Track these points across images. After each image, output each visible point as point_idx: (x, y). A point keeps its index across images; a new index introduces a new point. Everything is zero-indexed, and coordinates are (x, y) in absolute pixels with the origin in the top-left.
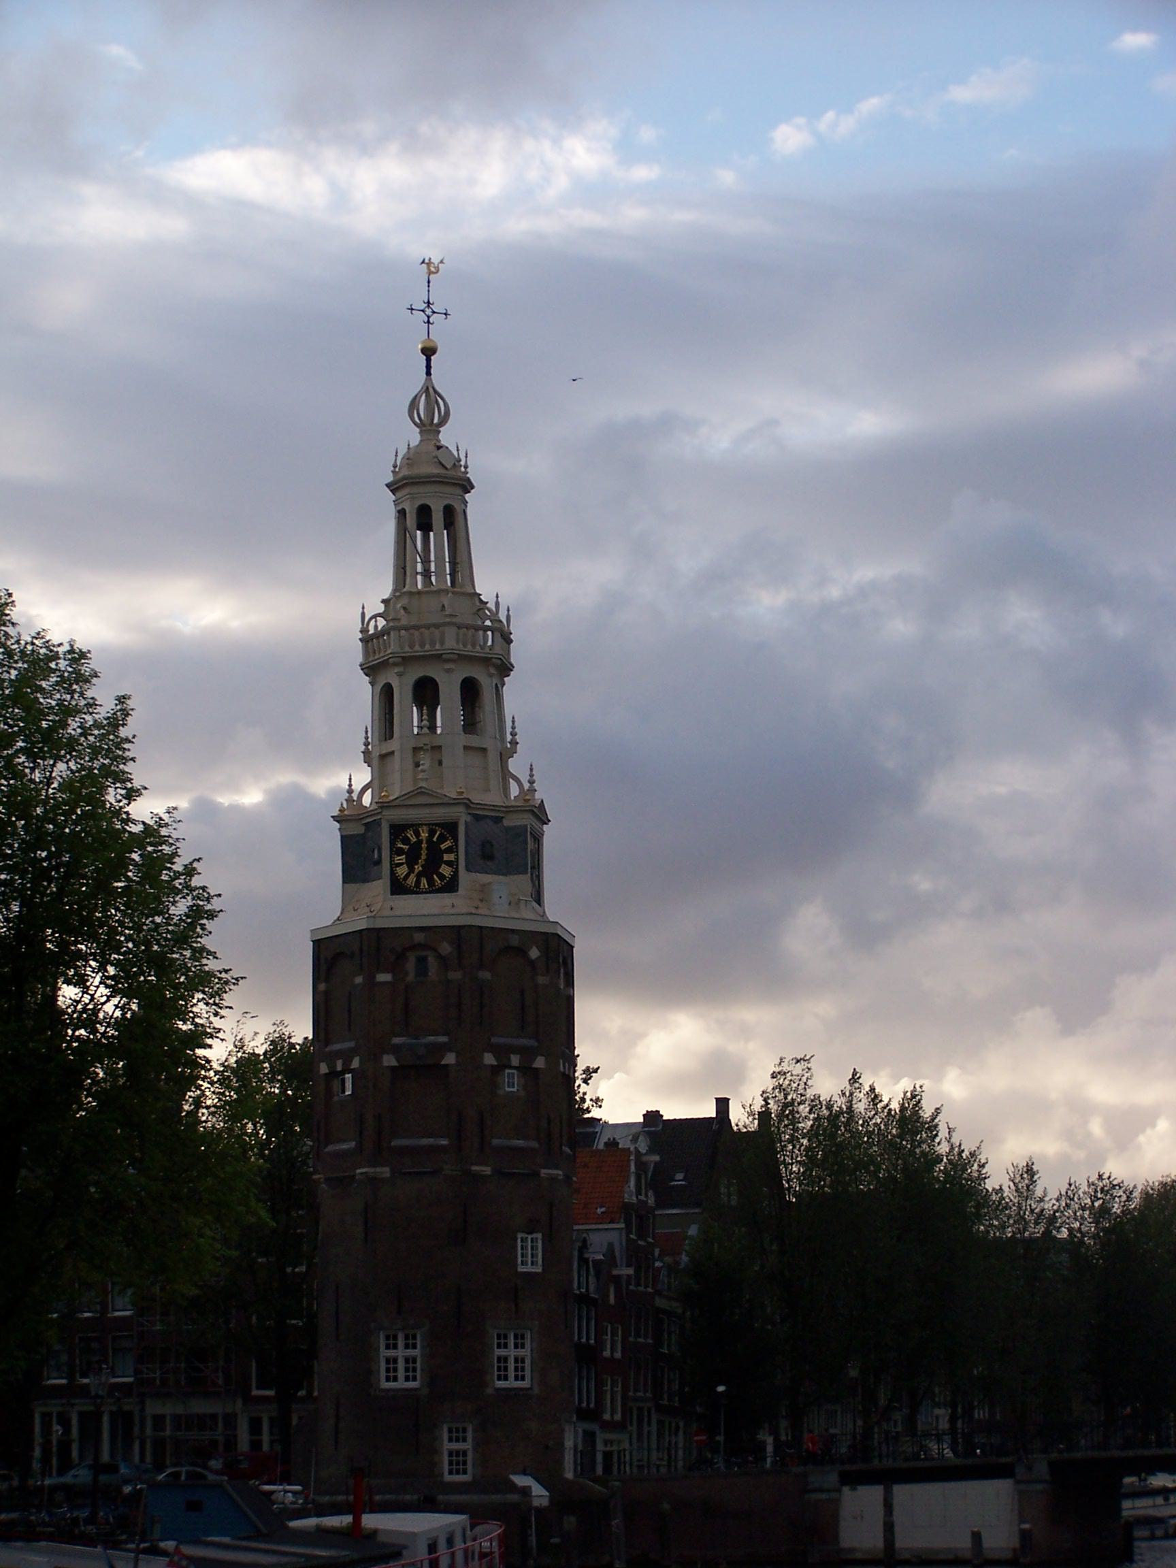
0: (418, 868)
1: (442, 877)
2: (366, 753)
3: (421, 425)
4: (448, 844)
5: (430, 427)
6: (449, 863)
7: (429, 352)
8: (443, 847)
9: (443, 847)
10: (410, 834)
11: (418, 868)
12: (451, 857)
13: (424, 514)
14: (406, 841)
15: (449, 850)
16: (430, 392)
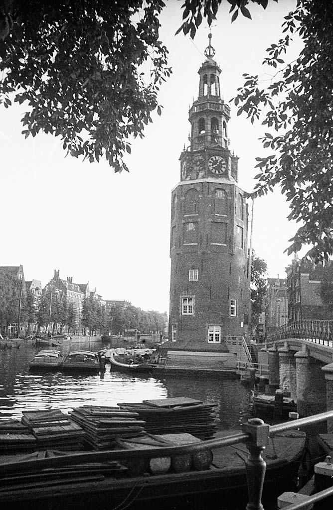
0: (214, 166)
1: (222, 171)
2: (189, 138)
3: (206, 55)
4: (224, 162)
5: (209, 56)
6: (224, 168)
7: (210, 36)
8: (223, 163)
9: (223, 163)
10: (213, 158)
11: (214, 166)
12: (225, 166)
13: (213, 76)
14: (212, 159)
15: (224, 164)
16: (210, 47)
